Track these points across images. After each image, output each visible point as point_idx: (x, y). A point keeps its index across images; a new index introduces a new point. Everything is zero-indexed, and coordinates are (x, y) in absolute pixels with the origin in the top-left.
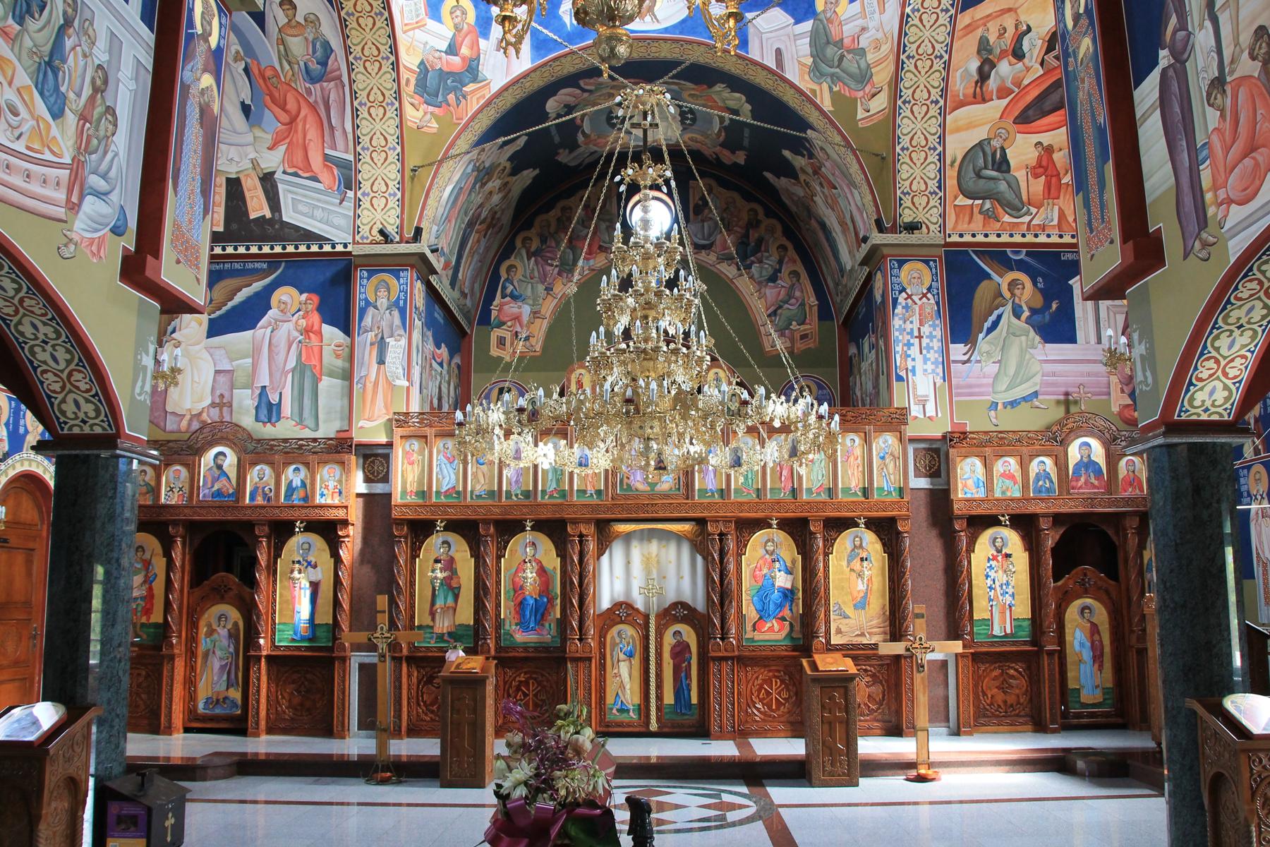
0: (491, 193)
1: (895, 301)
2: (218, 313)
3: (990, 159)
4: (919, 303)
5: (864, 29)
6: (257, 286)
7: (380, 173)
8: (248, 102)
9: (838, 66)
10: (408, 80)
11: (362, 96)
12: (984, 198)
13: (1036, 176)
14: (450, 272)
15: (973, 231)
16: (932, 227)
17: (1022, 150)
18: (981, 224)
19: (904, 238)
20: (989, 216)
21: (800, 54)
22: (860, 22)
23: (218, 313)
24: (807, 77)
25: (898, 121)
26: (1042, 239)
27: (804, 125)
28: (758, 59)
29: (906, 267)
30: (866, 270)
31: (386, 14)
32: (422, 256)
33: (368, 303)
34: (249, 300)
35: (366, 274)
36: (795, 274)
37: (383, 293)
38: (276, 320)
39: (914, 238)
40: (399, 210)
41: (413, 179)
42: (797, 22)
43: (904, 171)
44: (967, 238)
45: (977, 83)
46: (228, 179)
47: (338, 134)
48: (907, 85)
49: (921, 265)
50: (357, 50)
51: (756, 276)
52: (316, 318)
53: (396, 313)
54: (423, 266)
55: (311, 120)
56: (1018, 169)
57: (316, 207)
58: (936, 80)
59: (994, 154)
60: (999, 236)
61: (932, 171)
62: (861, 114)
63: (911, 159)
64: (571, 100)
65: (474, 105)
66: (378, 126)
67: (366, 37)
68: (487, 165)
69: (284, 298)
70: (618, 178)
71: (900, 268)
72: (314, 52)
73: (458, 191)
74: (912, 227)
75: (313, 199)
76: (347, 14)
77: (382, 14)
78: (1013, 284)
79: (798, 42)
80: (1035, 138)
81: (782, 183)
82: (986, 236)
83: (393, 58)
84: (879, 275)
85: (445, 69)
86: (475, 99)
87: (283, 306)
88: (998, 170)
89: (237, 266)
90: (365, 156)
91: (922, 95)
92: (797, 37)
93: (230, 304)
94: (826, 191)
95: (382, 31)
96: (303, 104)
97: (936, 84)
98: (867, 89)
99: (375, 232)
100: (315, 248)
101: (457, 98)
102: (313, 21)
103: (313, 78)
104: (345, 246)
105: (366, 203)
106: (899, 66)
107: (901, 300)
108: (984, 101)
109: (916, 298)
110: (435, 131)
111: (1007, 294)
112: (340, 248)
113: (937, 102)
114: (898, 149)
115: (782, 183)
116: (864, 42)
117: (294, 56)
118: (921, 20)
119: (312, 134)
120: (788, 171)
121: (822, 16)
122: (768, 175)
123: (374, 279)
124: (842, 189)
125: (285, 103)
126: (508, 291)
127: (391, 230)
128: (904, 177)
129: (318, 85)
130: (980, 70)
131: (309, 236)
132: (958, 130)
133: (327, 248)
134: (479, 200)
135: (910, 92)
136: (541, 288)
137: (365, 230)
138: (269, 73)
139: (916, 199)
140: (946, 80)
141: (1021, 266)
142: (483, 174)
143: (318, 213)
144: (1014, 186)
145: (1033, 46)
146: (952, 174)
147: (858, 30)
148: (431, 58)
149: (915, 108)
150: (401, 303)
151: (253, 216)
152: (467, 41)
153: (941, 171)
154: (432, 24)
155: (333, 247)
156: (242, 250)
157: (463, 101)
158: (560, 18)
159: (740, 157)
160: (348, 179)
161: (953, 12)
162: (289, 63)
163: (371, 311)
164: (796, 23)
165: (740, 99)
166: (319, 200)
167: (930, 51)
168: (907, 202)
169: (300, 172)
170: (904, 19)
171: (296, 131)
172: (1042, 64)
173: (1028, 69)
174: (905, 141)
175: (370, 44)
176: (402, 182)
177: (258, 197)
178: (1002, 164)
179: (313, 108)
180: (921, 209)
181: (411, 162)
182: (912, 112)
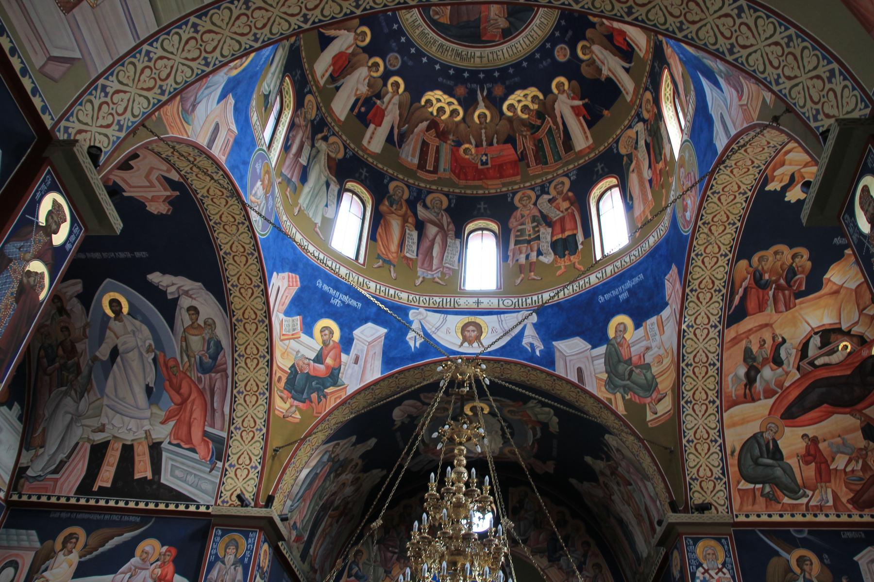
0: (344, 484)
1: (693, 575)
2: (88, 557)
3: (764, 449)
4: (716, 577)
5: (648, 349)
6: (128, 536)
7: (247, 449)
8: (152, 385)
9: (629, 379)
10: (280, 379)
11: (241, 386)
12: (763, 483)
13: (807, 463)
14: (302, 546)
15: (759, 513)
16: (720, 509)
17: (791, 441)
18: (764, 506)
19: (696, 517)
20: (771, 499)
21: (597, 371)
22: (644, 343)
23: (88, 557)
24: (603, 389)
25: (683, 417)
26: (821, 518)
27: (602, 430)
28: (563, 375)
29: (701, 544)
30: (663, 551)
31: (267, 322)
32: (270, 520)
33: (217, 558)
34: (117, 547)
35: (220, 533)
36: (597, 566)
37: (231, 550)
38: (136, 568)
39: (706, 517)
40: (257, 481)
41: (273, 459)
42: (594, 347)
43: (692, 460)
44: (753, 518)
45: (746, 385)
46: (124, 446)
47: (218, 415)
48: (688, 388)
49: (713, 543)
50: (241, 349)
51: (564, 567)
52: (170, 568)
53: (240, 569)
54: (269, 529)
55: (198, 403)
56: (790, 457)
57: (191, 473)
58: (711, 383)
59: (767, 444)
60: (781, 516)
61: (715, 460)
62: (649, 416)
63: (696, 450)
64: (413, 411)
65: (332, 403)
66: (250, 412)
67: (249, 339)
68: (342, 458)
69: (147, 549)
70: (435, 435)
71: (695, 544)
72: (208, 349)
73: (313, 477)
74: (704, 508)
75: (189, 466)
76: (237, 320)
77: (263, 322)
78: (801, 561)
79: (596, 362)
80: (801, 431)
81: (585, 487)
83: (268, 357)
84: (676, 553)
85: (312, 373)
86: (333, 399)
87: (145, 555)
89: (115, 518)
90: (237, 435)
91: (700, 395)
92: (594, 359)
93: (101, 550)
94: (622, 488)
95: (263, 335)
96: (194, 389)
97: (712, 387)
98: (654, 396)
99: (234, 497)
100: (182, 508)
101: (319, 397)
102: (210, 324)
103: (204, 369)
104: (208, 507)
105: (231, 473)
106: (679, 372)
107: (698, 574)
109: (712, 573)
110: (298, 421)
111: (797, 570)
112: (203, 509)
113: (714, 402)
114: (684, 441)
115: (585, 487)
116: (648, 359)
117: (192, 351)
118: (695, 335)
119: (197, 414)
120: (590, 475)
121: (613, 342)
122: (573, 481)
123: (226, 538)
124: (637, 484)
125: (180, 387)
126: (354, 572)
127: (248, 496)
128: (692, 465)
129: (207, 376)
130: (747, 375)
131: (179, 497)
132: (734, 425)
133: (192, 508)
134: (333, 488)
135: (691, 393)
136: (381, 570)
137: (226, 495)
138: (171, 363)
139: (703, 484)
140: (720, 383)
141: (804, 543)
142: (337, 466)
143: (191, 479)
144: (788, 471)
145: (789, 354)
146: (733, 462)
147: (643, 349)
148: (301, 363)
149: (696, 407)
150: (246, 560)
151: (137, 476)
152: (332, 354)
153: (724, 459)
154: (304, 338)
155: (198, 507)
156: (121, 504)
157: (324, 400)
158: (407, 343)
159: (550, 467)
160: (220, 451)
161: (720, 327)
162: (188, 356)
163: (219, 565)
164: (592, 348)
165: (549, 413)
166: (193, 468)
167: (705, 360)
168: (696, 486)
169: (182, 444)
170: (681, 334)
171: (185, 410)
172: (798, 369)
173: (787, 373)
174: (690, 435)
175: (251, 345)
176: (263, 458)
177: (144, 462)
178: (776, 454)
179: (201, 393)
180: (709, 492)
181: (275, 443)
182: (694, 410)
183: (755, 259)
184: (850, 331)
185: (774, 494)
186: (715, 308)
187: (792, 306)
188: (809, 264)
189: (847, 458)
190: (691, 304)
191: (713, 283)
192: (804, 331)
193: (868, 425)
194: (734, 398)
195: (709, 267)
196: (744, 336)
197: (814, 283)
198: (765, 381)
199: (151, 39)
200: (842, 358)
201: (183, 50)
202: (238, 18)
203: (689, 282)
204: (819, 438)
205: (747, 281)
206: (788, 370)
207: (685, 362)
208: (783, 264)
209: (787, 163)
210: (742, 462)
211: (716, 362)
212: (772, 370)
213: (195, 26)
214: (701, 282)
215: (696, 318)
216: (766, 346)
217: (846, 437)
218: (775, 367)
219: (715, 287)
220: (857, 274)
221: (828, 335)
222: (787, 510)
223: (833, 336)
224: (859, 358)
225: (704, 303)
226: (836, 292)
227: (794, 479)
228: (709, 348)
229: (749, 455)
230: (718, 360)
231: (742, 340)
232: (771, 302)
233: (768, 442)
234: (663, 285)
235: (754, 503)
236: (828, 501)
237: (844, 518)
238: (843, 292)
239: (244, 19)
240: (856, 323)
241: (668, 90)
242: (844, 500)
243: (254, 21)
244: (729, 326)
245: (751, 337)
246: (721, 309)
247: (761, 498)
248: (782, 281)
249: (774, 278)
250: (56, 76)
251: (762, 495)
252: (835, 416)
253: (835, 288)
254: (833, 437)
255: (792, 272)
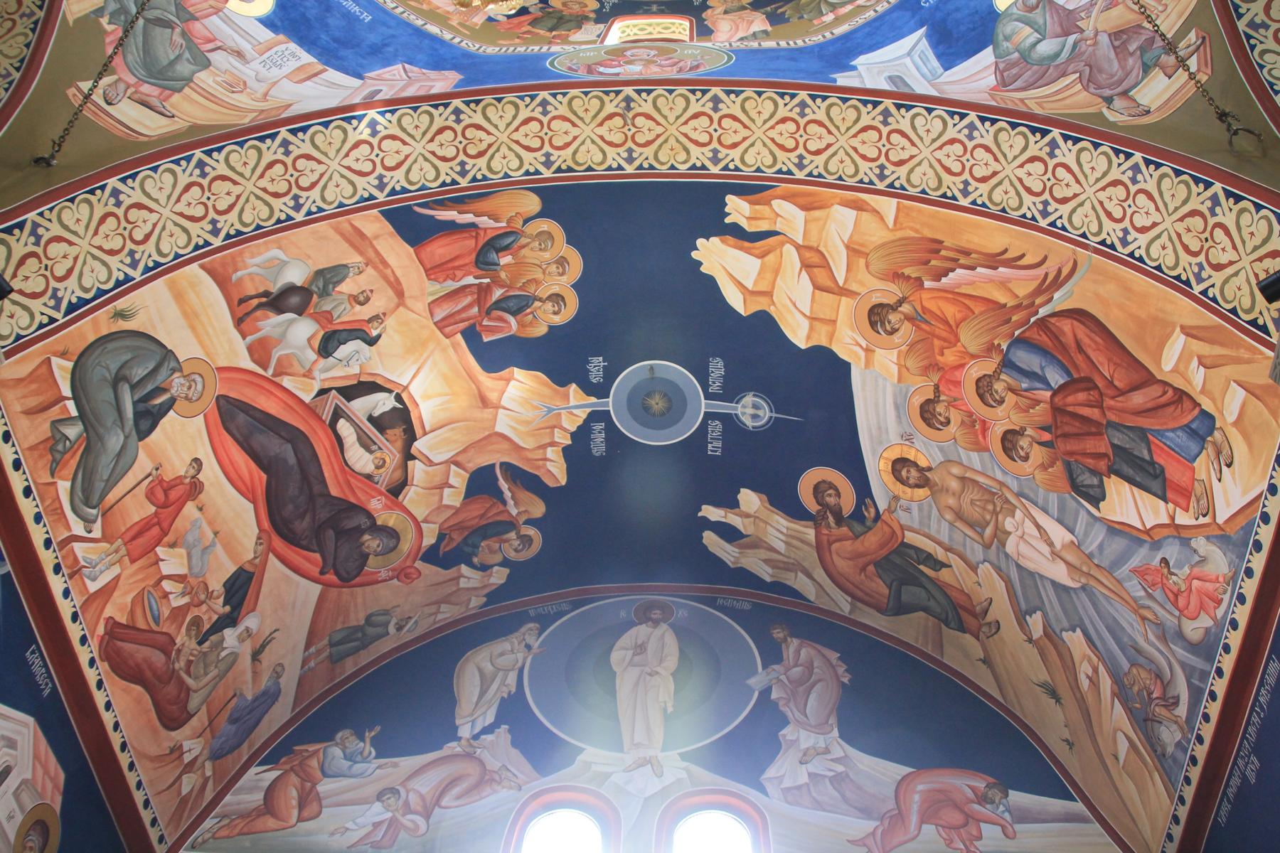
3: (150, 387)
5: (239, 54)
12: (82, 416)
13: (150, 495)
17: (183, 440)
18: (33, 439)
20: (53, 447)
22: (245, 46)
25: (165, 164)
26: (56, 584)
43: (76, 214)
45: (266, 294)
56: (151, 454)
58: (255, 213)
59: (160, 390)
60: (27, 492)
61: (96, 277)
63: (102, 220)
80: (205, 452)
82: (17, 465)
88: (138, 415)
91: (223, 194)
97: (247, 218)
98: (146, 88)
106: (263, 130)
108: (239, 322)
114: (113, 182)
118: (356, 145)
128: (68, 217)
130: (291, 289)
132: (179, 296)
135: (222, 169)
139: (32, 262)
140: (260, 233)
144: (124, 461)
147: (230, 44)
149: (196, 191)
153: (102, 297)
161: (381, 197)
172: (323, 392)
173: (308, 374)
174: (132, 194)
178: (148, 419)
183: (546, 225)
184: (414, 458)
185: (64, 453)
186: (423, 175)
187: (447, 330)
188: (541, 330)
189: (183, 570)
190: (426, 118)
191: (481, 154)
192: (397, 371)
193: (250, 576)
194: (234, 277)
195: (516, 136)
196: (371, 254)
197: (495, 356)
198: (284, 334)
200: (357, 468)
203: (477, 102)
204: (202, 496)
205: (492, 224)
206: (316, 374)
207: (291, 138)
208: (536, 282)
209: (817, 213)
210: (110, 346)
211: (304, 210)
212: (309, 340)
214: (478, 127)
215: (394, 137)
216: (358, 308)
217: (219, 549)
218: (316, 344)
219: (470, 162)
220: (527, 423)
221: (400, 422)
222: (42, 500)
223: (397, 433)
224: (363, 498)
225: (433, 146)
226: (484, 402)
227: (111, 483)
228: (331, 185)
229: (128, 356)
230: (309, 213)
231: (361, 253)
232: (451, 285)
233: (165, 390)
234: (388, 63)
235: (29, 412)
236: (94, 580)
237: (74, 632)
238: (487, 413)
240: (430, 463)
241: (635, 30)
242: (109, 611)
244: (388, 215)
245: (370, 270)
246: (423, 188)
247: (48, 425)
248: (498, 293)
249: (503, 275)
251: (55, 424)
252: (251, 506)
253: (493, 396)
254: (210, 523)
255: (518, 305)
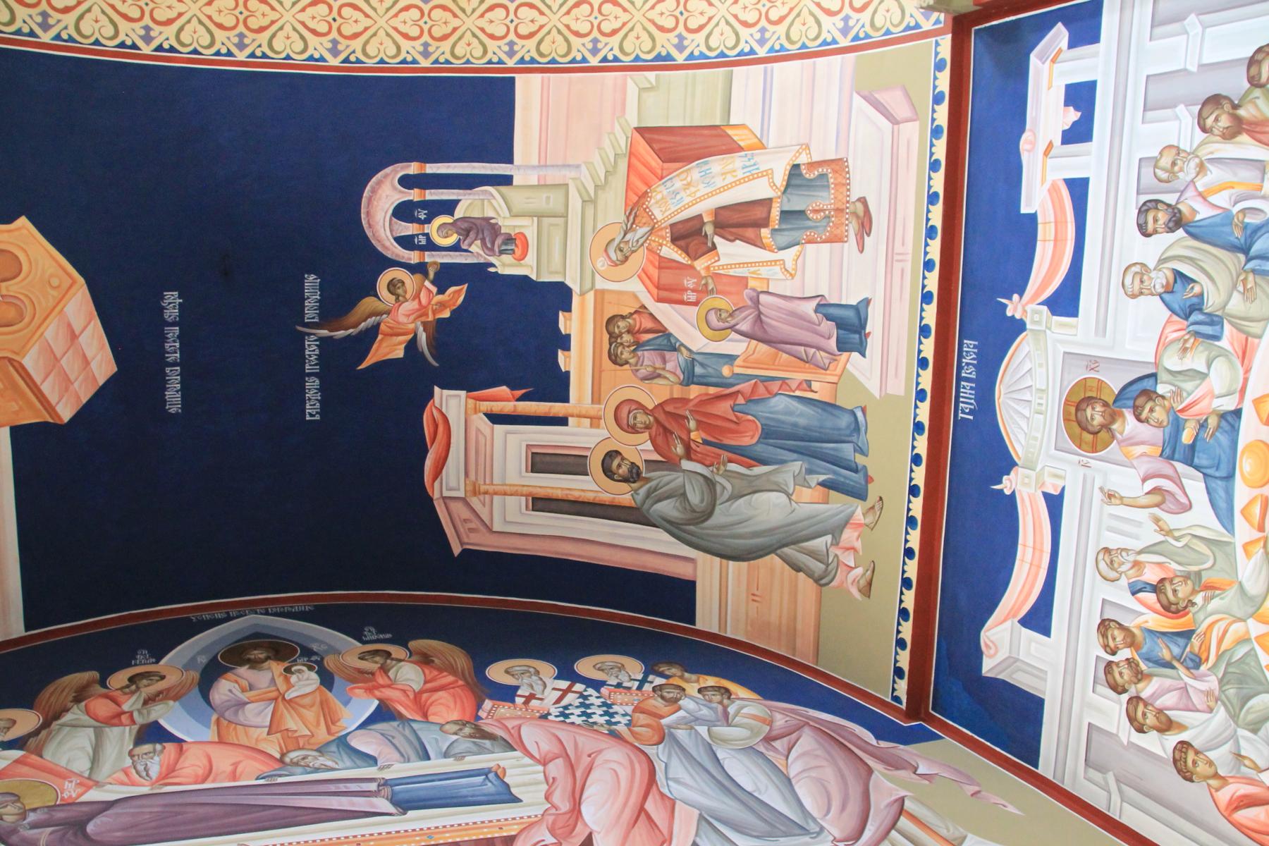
199: (747, 59)
201: (710, 19)
202: (614, 32)
213: (680, 47)
239: (606, 27)
243: (591, 18)
250: (899, 94)
